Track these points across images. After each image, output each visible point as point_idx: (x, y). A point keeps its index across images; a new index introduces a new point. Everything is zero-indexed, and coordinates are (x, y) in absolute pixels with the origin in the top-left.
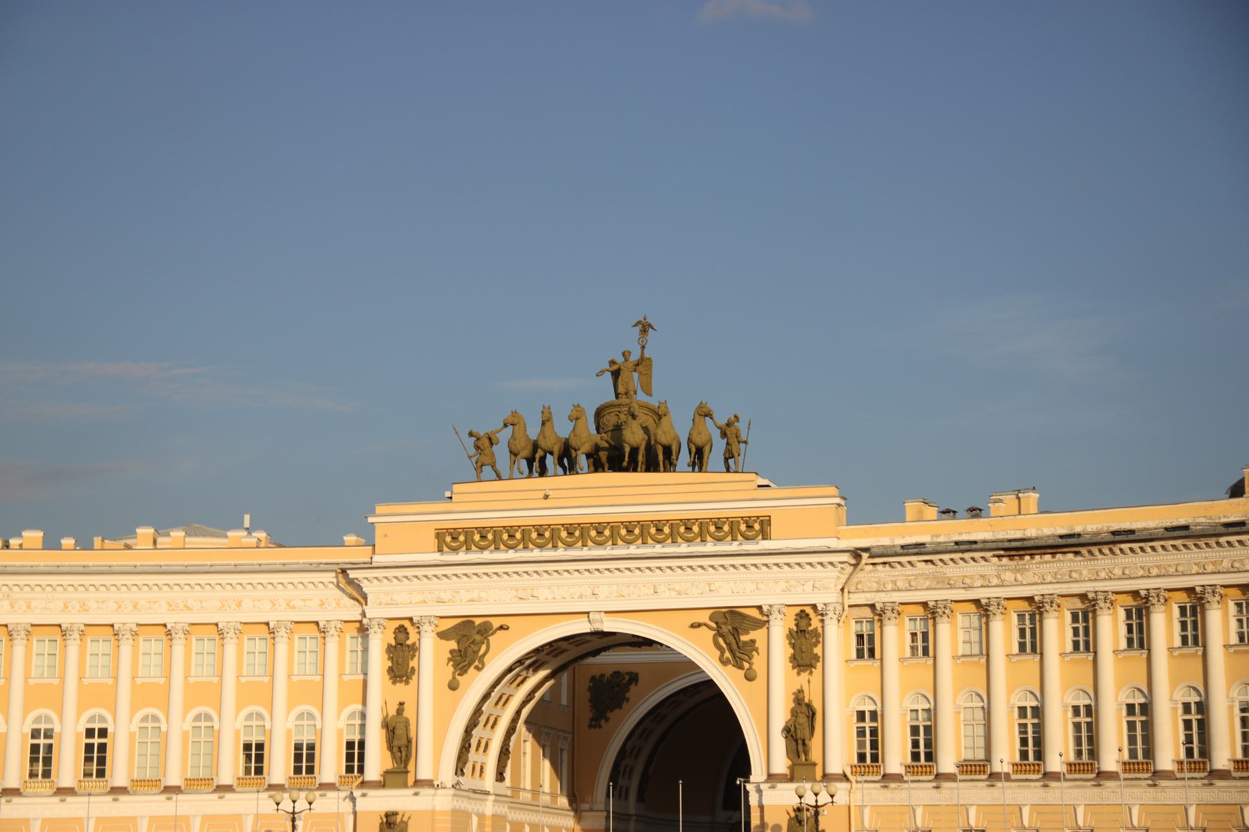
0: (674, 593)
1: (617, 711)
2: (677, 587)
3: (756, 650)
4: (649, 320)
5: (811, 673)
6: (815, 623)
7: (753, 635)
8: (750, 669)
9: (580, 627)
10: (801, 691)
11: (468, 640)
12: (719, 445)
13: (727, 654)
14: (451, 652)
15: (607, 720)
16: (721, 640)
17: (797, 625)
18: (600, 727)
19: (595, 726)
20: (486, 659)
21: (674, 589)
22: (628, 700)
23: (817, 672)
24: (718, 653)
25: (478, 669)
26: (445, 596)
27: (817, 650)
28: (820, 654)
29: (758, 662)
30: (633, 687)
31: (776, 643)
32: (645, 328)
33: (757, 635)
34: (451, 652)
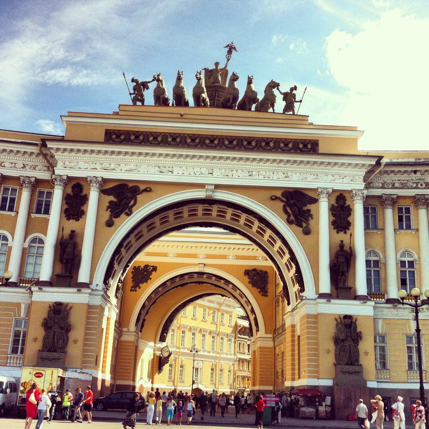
0: (261, 177)
1: (145, 284)
2: (264, 173)
3: (311, 216)
4: (235, 44)
5: (345, 233)
6: (348, 203)
7: (309, 207)
8: (306, 227)
9: (200, 194)
10: (342, 242)
11: (122, 196)
12: (280, 104)
13: (292, 218)
14: (111, 202)
15: (140, 288)
16: (289, 210)
17: (337, 203)
18: (136, 291)
19: (133, 291)
20: (133, 209)
21: (262, 175)
22: (150, 279)
23: (349, 232)
24: (286, 216)
25: (128, 215)
26: (113, 166)
27: (350, 219)
28: (351, 221)
29: (312, 222)
30: (154, 273)
31: (323, 212)
32: (231, 49)
33: (311, 207)
34: (111, 202)
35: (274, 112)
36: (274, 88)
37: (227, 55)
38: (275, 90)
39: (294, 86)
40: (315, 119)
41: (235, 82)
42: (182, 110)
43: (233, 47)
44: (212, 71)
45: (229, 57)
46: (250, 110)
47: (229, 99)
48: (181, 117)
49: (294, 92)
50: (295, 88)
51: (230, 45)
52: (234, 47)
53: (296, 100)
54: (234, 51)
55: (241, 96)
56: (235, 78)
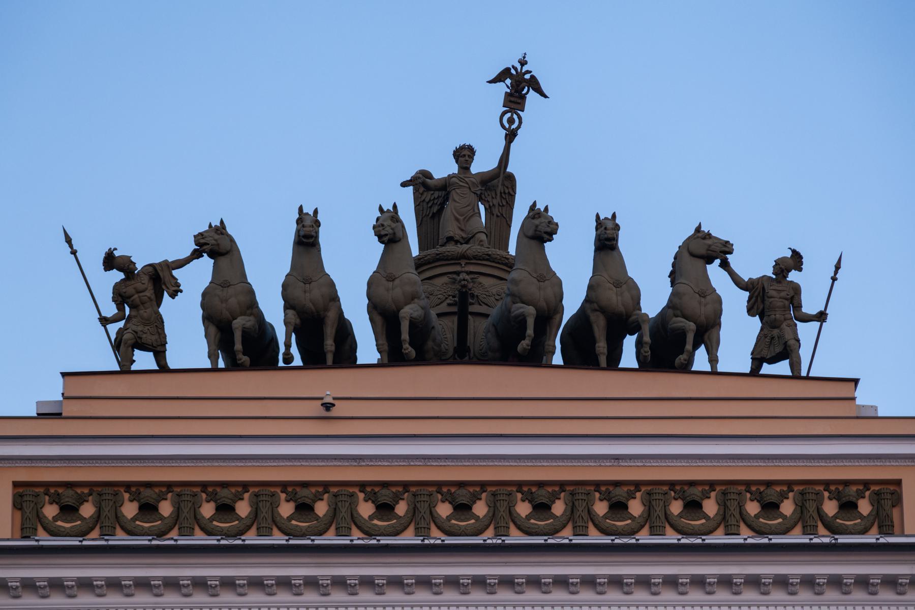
4: (535, 68)
32: (519, 86)
35: (714, 373)
36: (710, 261)
37: (504, 113)
38: (714, 271)
39: (789, 254)
40: (881, 396)
41: (547, 245)
42: (329, 383)
43: (527, 76)
44: (446, 186)
45: (511, 121)
46: (613, 363)
47: (521, 322)
48: (324, 413)
49: (793, 276)
50: (796, 260)
51: (513, 72)
52: (533, 77)
53: (804, 310)
54: (532, 97)
55: (572, 302)
56: (541, 229)
